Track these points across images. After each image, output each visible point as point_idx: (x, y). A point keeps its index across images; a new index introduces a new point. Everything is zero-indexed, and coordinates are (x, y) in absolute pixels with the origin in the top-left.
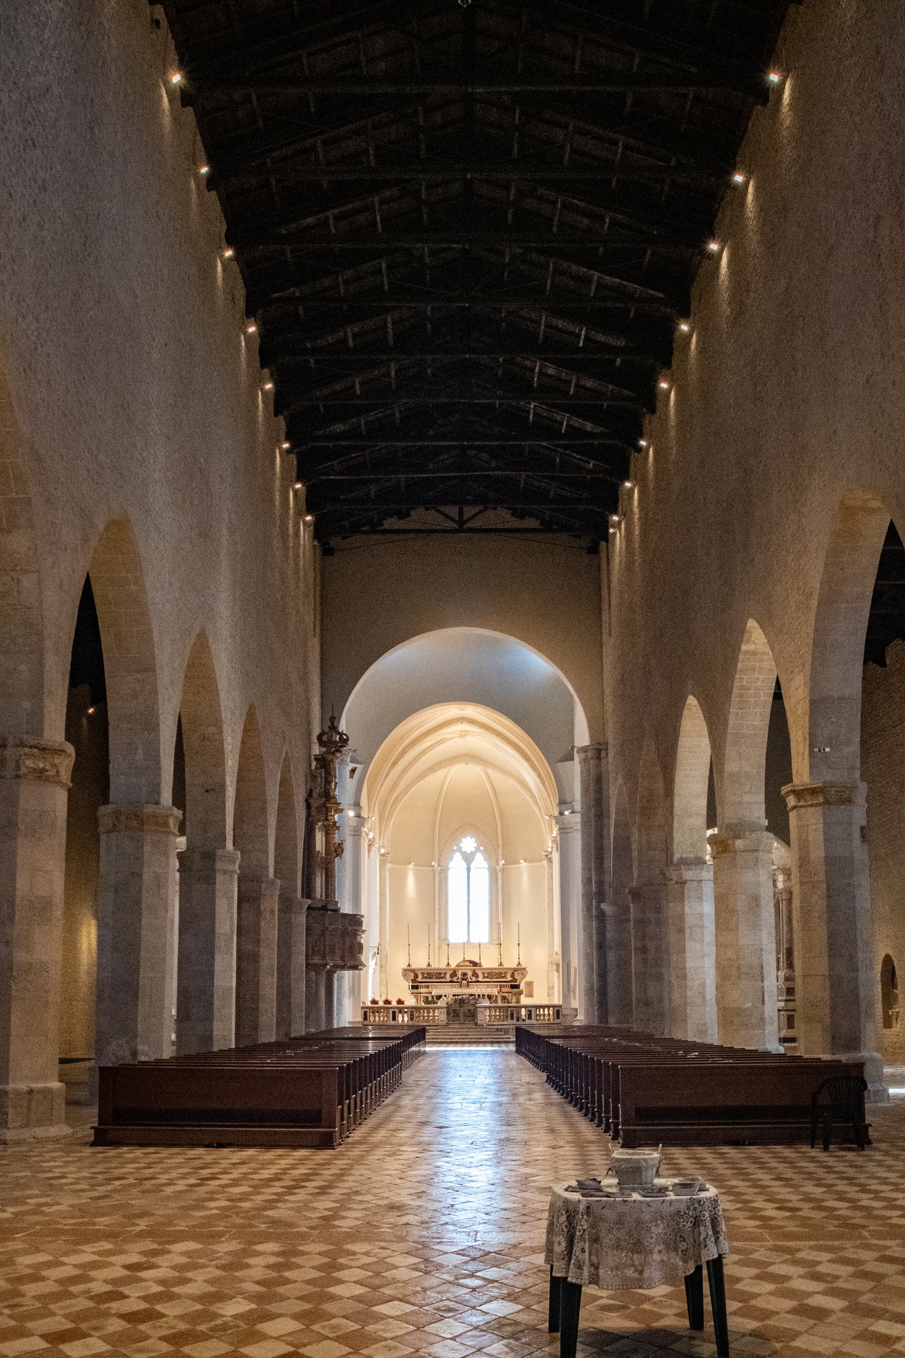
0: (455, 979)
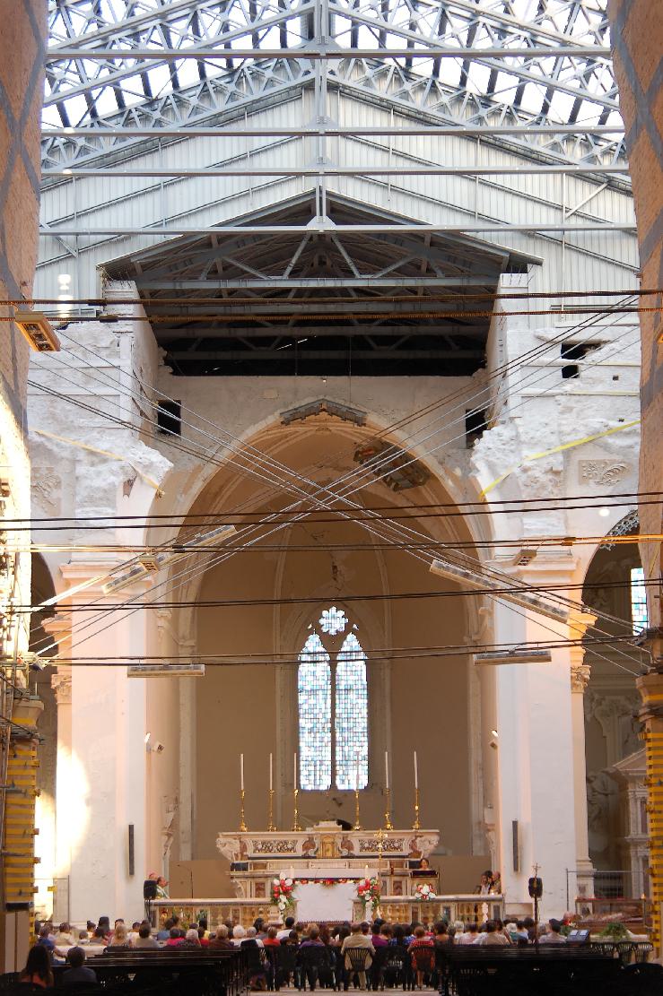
0: (311, 853)
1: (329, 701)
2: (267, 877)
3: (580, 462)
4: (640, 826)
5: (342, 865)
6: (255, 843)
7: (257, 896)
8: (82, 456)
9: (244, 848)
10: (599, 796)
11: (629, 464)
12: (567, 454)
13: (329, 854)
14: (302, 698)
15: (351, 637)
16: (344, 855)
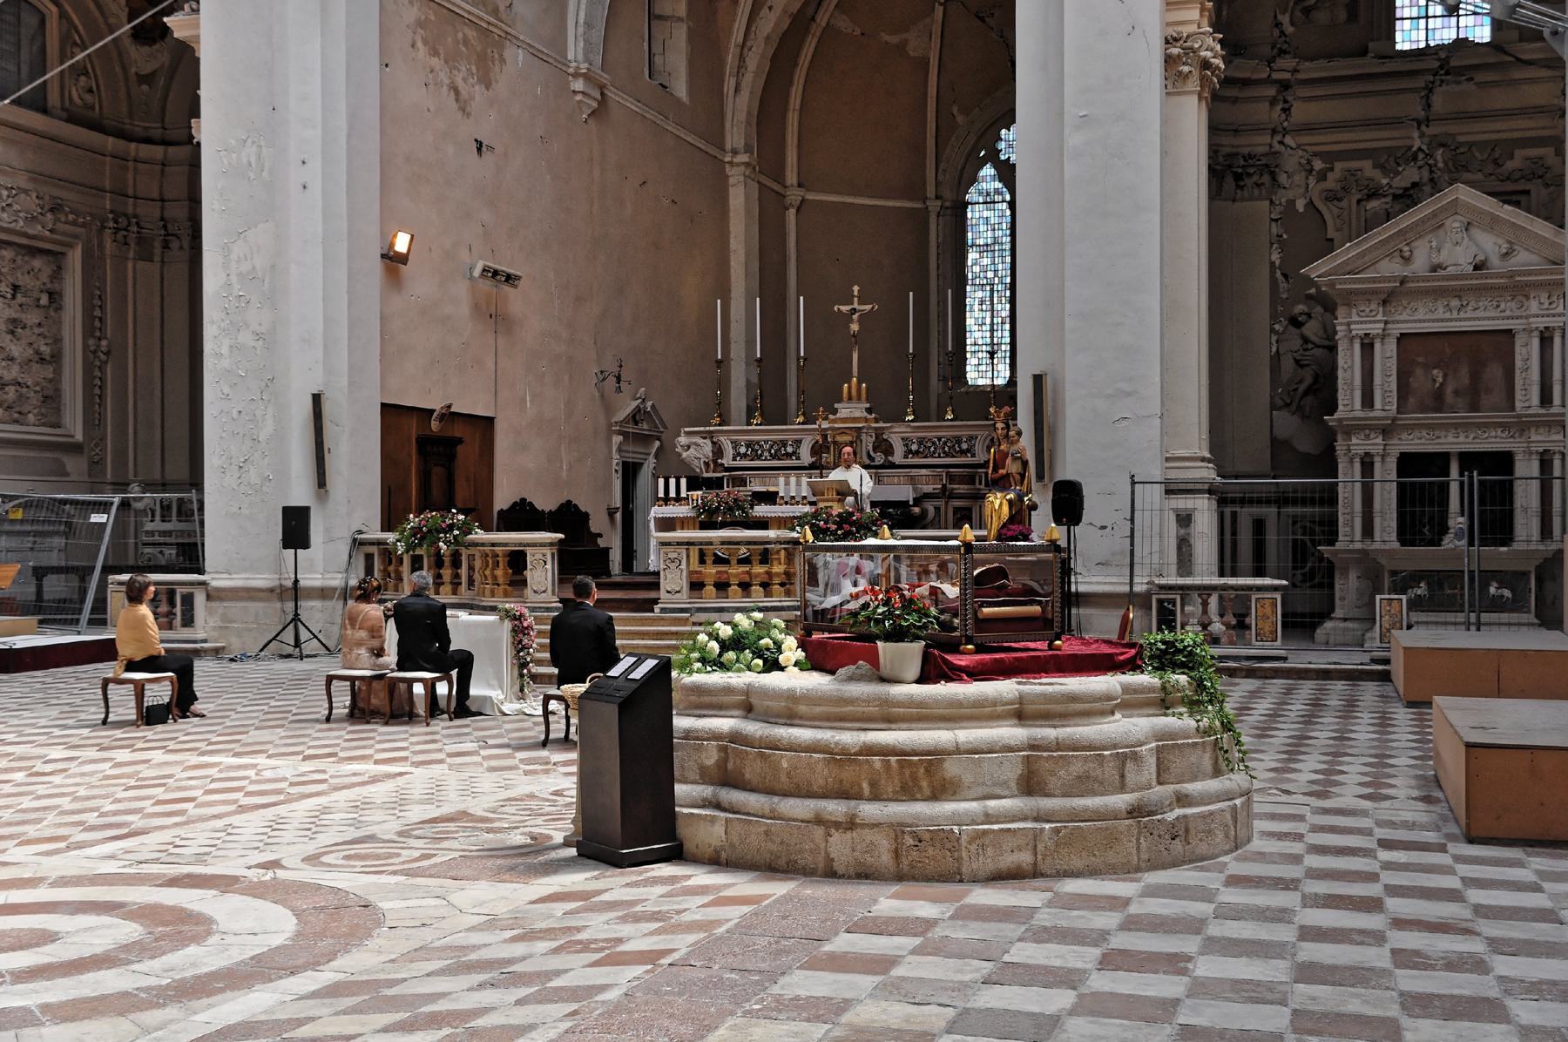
4: (1358, 394)
6: (735, 444)
9: (718, 452)
10: (1318, 352)
14: (972, 256)
16: (877, 463)
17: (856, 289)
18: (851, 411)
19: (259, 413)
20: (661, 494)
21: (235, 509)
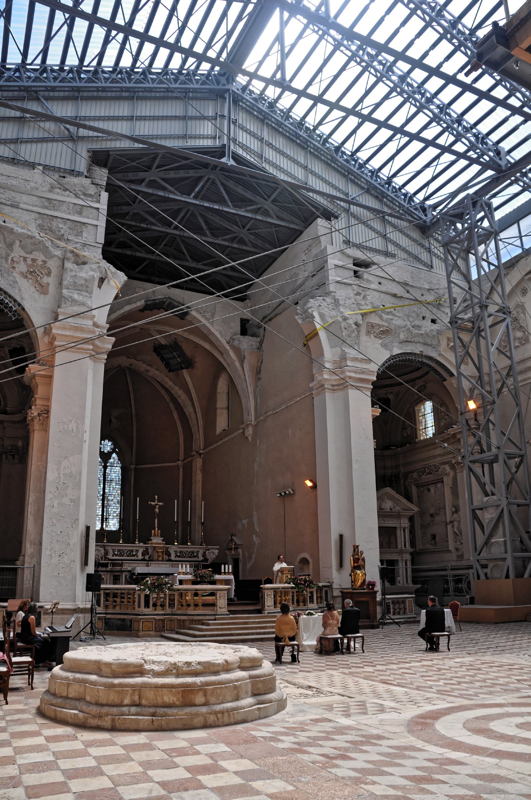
0: (147, 557)
1: (102, 486)
2: (122, 572)
3: (368, 323)
5: (168, 566)
6: (114, 550)
7: (114, 583)
8: (69, 255)
11: (391, 329)
12: (363, 315)
13: (160, 559)
15: (114, 455)
17: (156, 497)
18: (157, 540)
19: (70, 533)
20: (223, 571)
21: (56, 574)
